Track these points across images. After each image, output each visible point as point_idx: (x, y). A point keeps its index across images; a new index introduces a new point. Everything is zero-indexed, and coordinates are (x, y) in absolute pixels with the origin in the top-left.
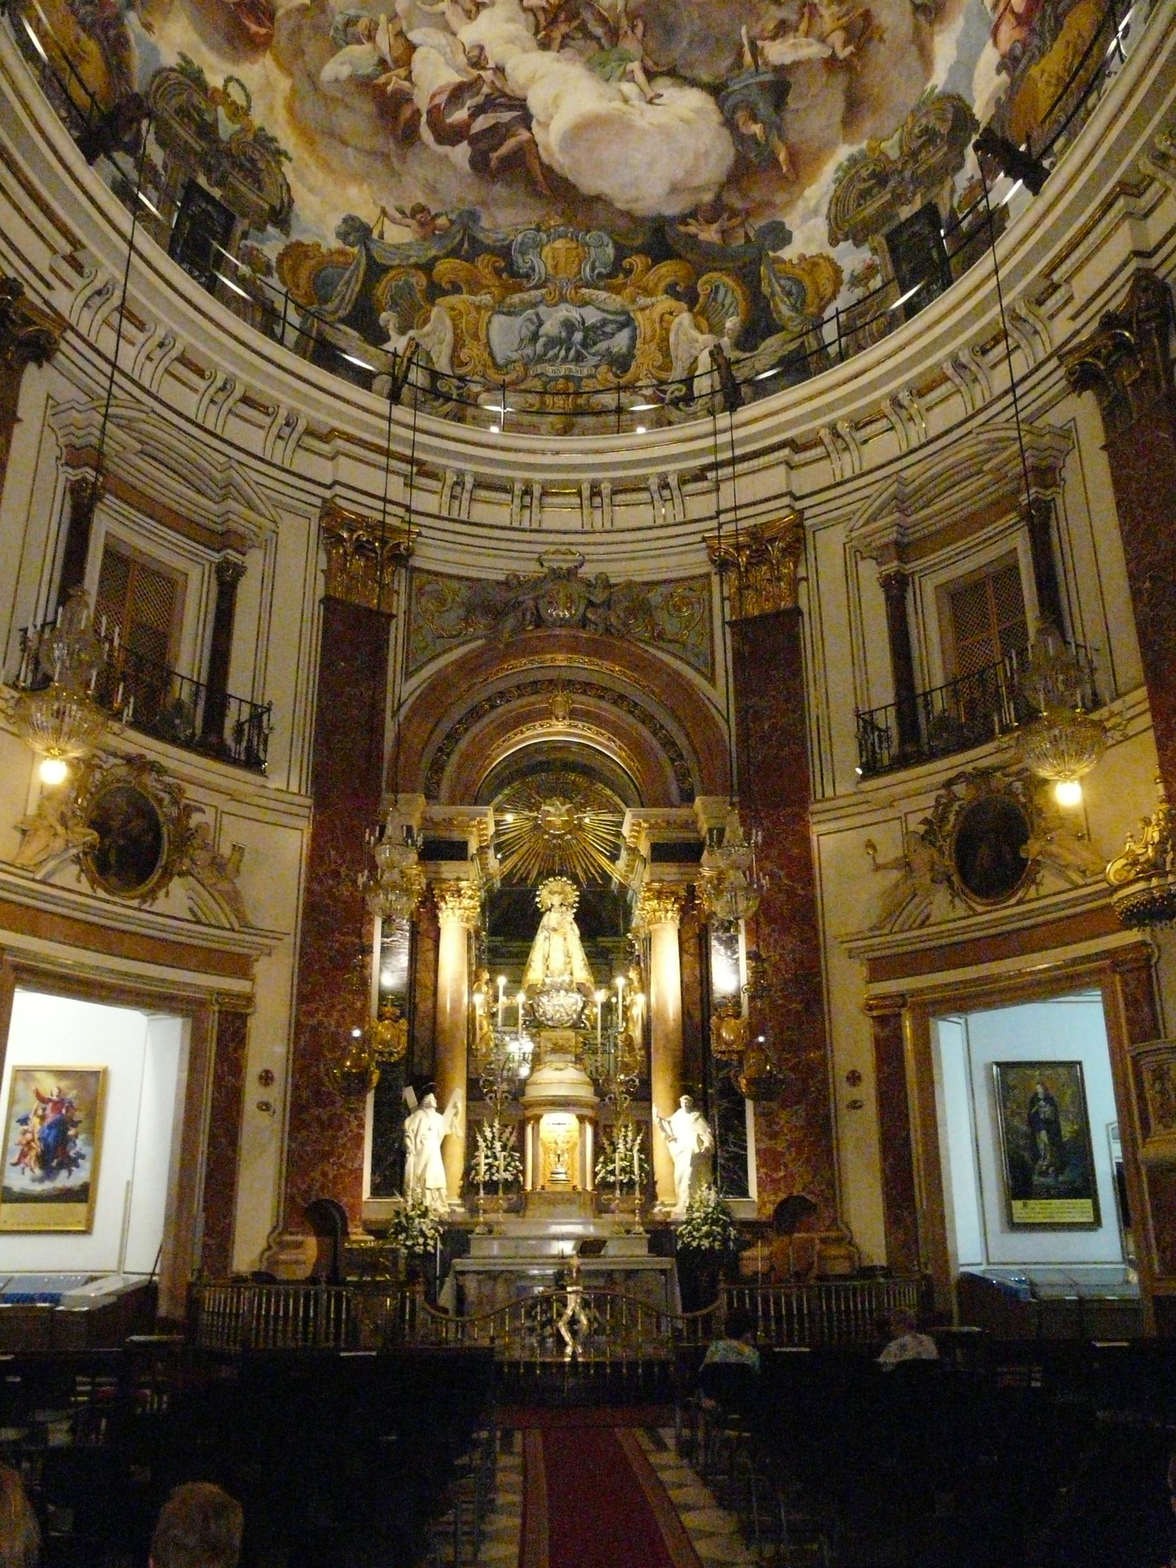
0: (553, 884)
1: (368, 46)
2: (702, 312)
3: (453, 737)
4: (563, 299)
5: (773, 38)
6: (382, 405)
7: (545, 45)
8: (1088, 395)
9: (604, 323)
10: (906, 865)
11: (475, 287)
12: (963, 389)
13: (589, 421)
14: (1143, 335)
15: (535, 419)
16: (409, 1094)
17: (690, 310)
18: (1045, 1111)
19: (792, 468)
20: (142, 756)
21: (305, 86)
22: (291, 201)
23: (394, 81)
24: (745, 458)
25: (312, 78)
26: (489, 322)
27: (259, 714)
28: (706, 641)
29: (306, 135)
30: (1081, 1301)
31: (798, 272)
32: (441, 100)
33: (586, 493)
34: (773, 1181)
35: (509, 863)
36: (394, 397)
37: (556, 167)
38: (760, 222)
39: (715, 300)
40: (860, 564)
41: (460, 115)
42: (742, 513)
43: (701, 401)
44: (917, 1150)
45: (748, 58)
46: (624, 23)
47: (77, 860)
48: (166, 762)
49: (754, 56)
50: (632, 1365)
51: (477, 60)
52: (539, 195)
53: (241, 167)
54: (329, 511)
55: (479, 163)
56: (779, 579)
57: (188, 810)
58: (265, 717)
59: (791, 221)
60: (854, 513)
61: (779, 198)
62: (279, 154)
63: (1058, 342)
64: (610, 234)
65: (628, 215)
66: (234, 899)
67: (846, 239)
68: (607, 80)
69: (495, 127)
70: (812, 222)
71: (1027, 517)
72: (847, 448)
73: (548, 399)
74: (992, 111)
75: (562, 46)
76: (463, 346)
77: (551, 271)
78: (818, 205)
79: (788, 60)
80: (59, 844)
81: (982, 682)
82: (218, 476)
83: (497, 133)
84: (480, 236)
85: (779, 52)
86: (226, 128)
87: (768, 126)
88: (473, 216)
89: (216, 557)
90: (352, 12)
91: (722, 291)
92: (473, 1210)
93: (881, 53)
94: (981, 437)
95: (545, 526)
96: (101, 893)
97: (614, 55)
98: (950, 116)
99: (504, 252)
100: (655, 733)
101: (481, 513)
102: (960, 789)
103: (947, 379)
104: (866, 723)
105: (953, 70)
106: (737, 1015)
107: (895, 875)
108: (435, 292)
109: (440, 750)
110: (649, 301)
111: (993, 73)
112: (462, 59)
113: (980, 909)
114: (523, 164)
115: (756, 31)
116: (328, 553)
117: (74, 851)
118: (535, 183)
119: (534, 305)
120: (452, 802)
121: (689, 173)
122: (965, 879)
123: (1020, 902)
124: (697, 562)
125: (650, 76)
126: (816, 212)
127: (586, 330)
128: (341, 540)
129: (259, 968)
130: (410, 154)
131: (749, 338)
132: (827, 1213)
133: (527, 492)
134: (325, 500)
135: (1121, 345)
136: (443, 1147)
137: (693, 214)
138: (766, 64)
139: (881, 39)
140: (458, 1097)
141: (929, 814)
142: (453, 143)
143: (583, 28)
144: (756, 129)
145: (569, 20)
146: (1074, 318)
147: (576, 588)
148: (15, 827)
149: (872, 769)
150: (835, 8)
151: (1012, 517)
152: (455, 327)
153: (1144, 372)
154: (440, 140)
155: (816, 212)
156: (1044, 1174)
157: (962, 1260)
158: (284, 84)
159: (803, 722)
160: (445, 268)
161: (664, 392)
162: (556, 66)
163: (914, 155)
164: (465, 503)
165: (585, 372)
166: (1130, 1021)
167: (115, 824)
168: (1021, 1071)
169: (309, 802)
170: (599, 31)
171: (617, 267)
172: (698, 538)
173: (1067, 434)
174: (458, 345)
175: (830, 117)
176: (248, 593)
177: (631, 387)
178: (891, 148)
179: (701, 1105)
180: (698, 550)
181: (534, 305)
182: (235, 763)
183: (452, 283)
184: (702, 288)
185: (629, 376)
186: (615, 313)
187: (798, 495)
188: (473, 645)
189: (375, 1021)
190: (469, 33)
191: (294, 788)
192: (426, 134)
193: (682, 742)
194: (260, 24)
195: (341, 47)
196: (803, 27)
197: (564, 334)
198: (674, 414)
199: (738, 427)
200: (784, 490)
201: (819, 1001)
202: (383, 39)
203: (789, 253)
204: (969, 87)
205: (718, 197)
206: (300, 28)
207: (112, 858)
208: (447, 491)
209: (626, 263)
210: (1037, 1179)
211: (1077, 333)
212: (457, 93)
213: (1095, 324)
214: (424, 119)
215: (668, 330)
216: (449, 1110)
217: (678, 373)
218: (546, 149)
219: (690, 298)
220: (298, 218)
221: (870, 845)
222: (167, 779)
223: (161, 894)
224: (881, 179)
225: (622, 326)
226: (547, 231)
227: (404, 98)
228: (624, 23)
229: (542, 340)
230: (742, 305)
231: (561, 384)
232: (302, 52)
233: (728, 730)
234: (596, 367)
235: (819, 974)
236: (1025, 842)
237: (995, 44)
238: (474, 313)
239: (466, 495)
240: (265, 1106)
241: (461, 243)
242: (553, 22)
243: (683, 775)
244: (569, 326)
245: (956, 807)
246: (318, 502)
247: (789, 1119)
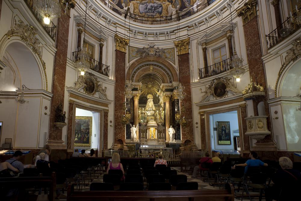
0: (150, 95)
2: (173, 5)
3: (135, 72)
4: (151, 2)
6: (124, 19)
8: (241, 17)
9: (158, 6)
10: (206, 92)
12: (218, 17)
13: (155, 22)
14: (252, 6)
15: (147, 22)
16: (131, 125)
17: (171, 4)
18: (224, 128)
19: (188, 30)
20: (91, 73)
24: (181, 29)
26: (139, 6)
27: (107, 67)
28: (174, 58)
30: (229, 154)
33: (155, 34)
34: (185, 138)
35: (142, 93)
36: (125, 17)
39: (176, 2)
40: (199, 46)
42: (180, 38)
43: (173, 19)
44: (206, 133)
47: (83, 88)
48: (95, 74)
50: (172, 162)
54: (116, 36)
56: (186, 48)
57: (98, 82)
58: (108, 68)
60: (199, 37)
63: (235, 9)
66: (105, 95)
71: (228, 38)
72: (197, 27)
73: (149, 19)
76: (135, 10)
80: (81, 86)
81: (225, 62)
82: (99, 29)
89: (99, 43)
91: (177, 1)
92: (140, 141)
94: (221, 25)
95: (148, 39)
96: (86, 94)
100: (166, 72)
101: (138, 37)
102: (215, 81)
103: (215, 15)
104: (200, 70)
106: (179, 114)
107: (204, 94)
109: (133, 74)
110: (164, 2)
113: (218, 99)
116: (116, 43)
117: (83, 87)
119: (146, 3)
120: (135, 82)
122: (215, 94)
123: (225, 97)
124: (172, 46)
127: (154, 7)
128: (118, 41)
129: (109, 106)
131: (181, 9)
132: (192, 142)
133: (146, 34)
134: (115, 34)
135: (248, 8)
136: (136, 132)
140: (138, 125)
141: (210, 84)
146: (239, 4)
147: (153, 49)
148: (74, 83)
149: (201, 78)
151: (225, 38)
152: (134, 6)
153: (252, 13)
156: (224, 137)
157: (212, 149)
159: (189, 70)
161: (167, 18)
164: (136, 35)
165: (154, 14)
166: (242, 115)
167: (88, 83)
168: (221, 123)
169: (115, 81)
172: (173, 42)
173: (236, 24)
174: (134, 9)
176: (104, 49)
177: (162, 17)
179: (173, 127)
181: (146, 3)
182: (104, 75)
185: (161, 16)
186: (159, 5)
187: (189, 35)
188: (138, 58)
189: (126, 114)
191: (113, 79)
193: (170, 74)
197: (151, 8)
198: (169, 22)
199: (180, 23)
200: (187, 34)
201: (192, 112)
207: (88, 88)
208: (133, 33)
210: (222, 138)
211: (239, 6)
213: (243, 5)
215: (168, 8)
216: (137, 127)
217: (169, 15)
221: (201, 89)
222: (95, 77)
223: (95, 94)
229: (148, 9)
230: (180, 4)
231: (151, 16)
233: (178, 72)
234: (156, 14)
235: (192, 108)
236: (226, 88)
239: (136, 34)
240: (111, 126)
243: (170, 79)
244: (152, 6)
245: (214, 83)
246: (114, 35)
247: (187, 129)
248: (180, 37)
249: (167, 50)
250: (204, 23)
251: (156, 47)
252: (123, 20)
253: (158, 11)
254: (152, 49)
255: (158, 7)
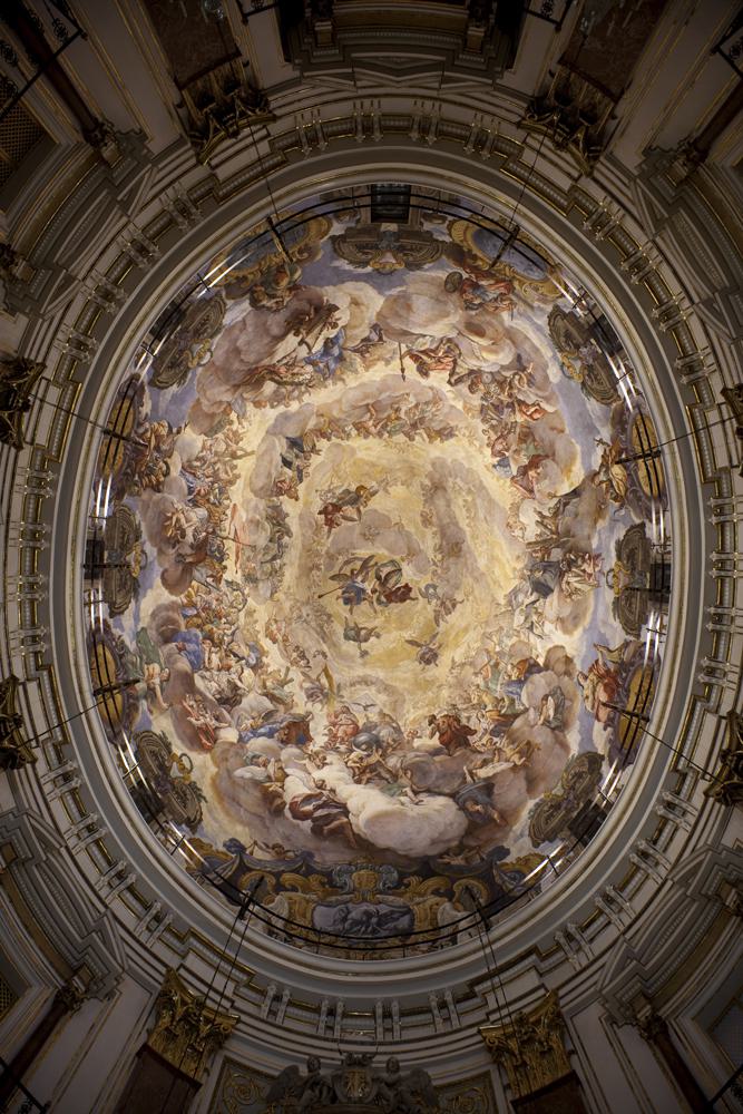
1: (263, 769)
4: (364, 900)
5: (481, 767)
7: (358, 782)
9: (392, 912)
11: (307, 889)
17: (450, 900)
21: (225, 775)
22: (201, 820)
23: (274, 787)
25: (229, 773)
26: (314, 909)
29: (221, 795)
31: (517, 867)
32: (299, 799)
33: (379, 1011)
37: (362, 835)
38: (489, 849)
41: (309, 808)
45: (469, 779)
46: (401, 773)
49: (472, 777)
51: (321, 785)
52: (352, 848)
53: (177, 793)
55: (317, 831)
59: (505, 845)
61: (498, 835)
62: (200, 797)
64: (396, 867)
65: (406, 856)
67: (544, 841)
68: (393, 796)
69: (328, 815)
70: (521, 840)
74: (609, 746)
75: (368, 781)
77: (358, 886)
78: (522, 831)
79: (491, 774)
83: (328, 818)
84: (315, 866)
85: (483, 773)
86: (175, 772)
87: (485, 805)
88: (311, 855)
90: (257, 753)
93: (539, 756)
97: (395, 785)
98: (586, 763)
99: (328, 874)
105: (580, 745)
108: (279, 888)
111: (603, 732)
112: (313, 784)
114: (342, 833)
115: (471, 766)
118: (349, 841)
121: (440, 834)
125: (416, 793)
126: (522, 835)
128: (171, 1005)
130: (276, 821)
137: (447, 853)
138: (479, 779)
139: (539, 749)
142: (303, 820)
143: (379, 775)
144: (479, 807)
145: (371, 772)
150: (511, 746)
152: (290, 909)
154: (295, 817)
155: (522, 835)
158: (213, 770)
160: (287, 876)
162: (363, 790)
163: (573, 788)
170: (388, 776)
171: (400, 883)
175: (520, 790)
178: (558, 791)
180: (474, 1052)
183: (293, 886)
184: (457, 888)
186: (400, 907)
190: (318, 774)
192: (287, 812)
194: (208, 740)
195: (248, 765)
196: (496, 758)
202: (271, 769)
203: (508, 860)
204: (593, 745)
205: (461, 842)
206: (228, 750)
209: (405, 881)
212: (308, 799)
213: (720, 764)
214: (287, 806)
215: (436, 914)
218: (357, 826)
219: (449, 895)
220: (202, 828)
224: (557, 807)
225: (404, 914)
226: (356, 866)
227: (280, 796)
228: (401, 773)
229: (350, 921)
232: (227, 760)
237: (599, 720)
238: (304, 903)
241: (301, 867)
242: (364, 772)
244: (368, 915)
248: (508, 1005)
249: (451, 1094)
250: (601, 920)
251: (380, 1061)
252: (228, 926)
253: (395, 928)
254: (357, 1069)
255: (395, 916)
